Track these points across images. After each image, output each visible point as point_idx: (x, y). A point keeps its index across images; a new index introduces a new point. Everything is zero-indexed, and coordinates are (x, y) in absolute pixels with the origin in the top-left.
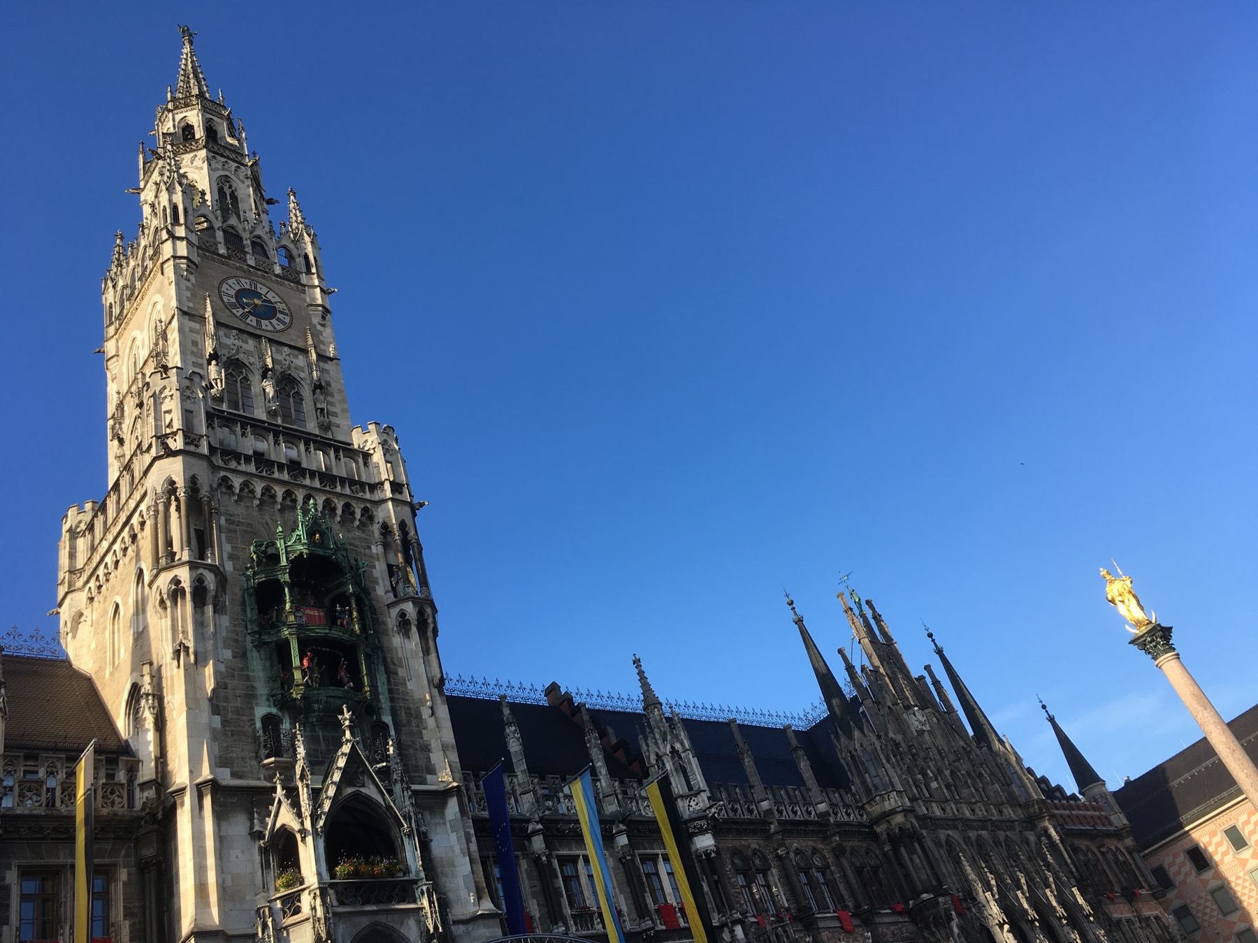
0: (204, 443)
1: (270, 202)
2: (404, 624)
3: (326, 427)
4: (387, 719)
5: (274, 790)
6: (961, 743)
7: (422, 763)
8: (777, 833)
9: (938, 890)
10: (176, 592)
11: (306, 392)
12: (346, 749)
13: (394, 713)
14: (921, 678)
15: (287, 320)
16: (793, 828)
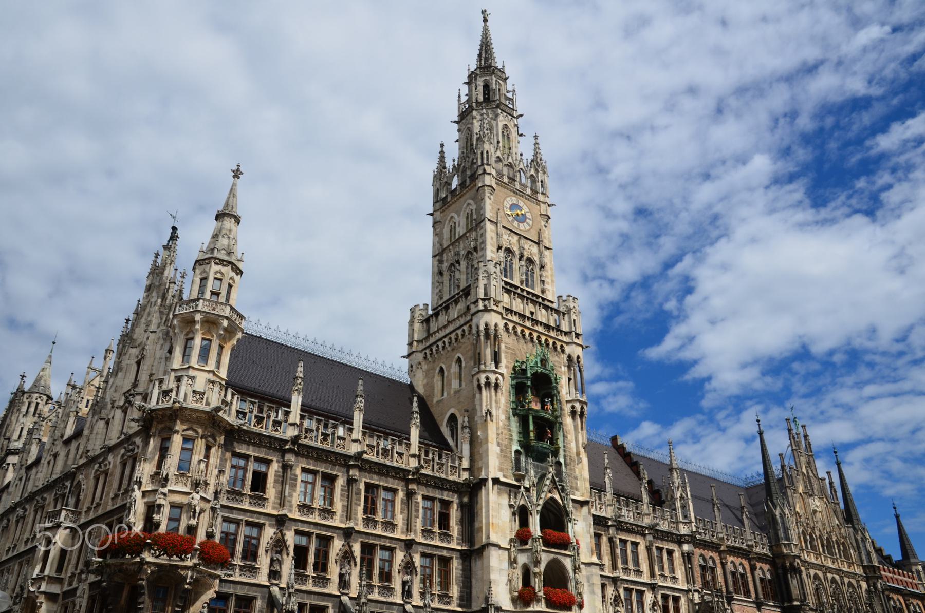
0: (501, 305)
1: (521, 135)
2: (573, 413)
3: (543, 291)
4: (562, 460)
5: (519, 487)
6: (837, 522)
7: (574, 485)
8: (724, 551)
9: (803, 600)
10: (488, 384)
11: (537, 269)
12: (550, 476)
13: (565, 456)
14: (824, 479)
15: (531, 223)
16: (733, 551)
